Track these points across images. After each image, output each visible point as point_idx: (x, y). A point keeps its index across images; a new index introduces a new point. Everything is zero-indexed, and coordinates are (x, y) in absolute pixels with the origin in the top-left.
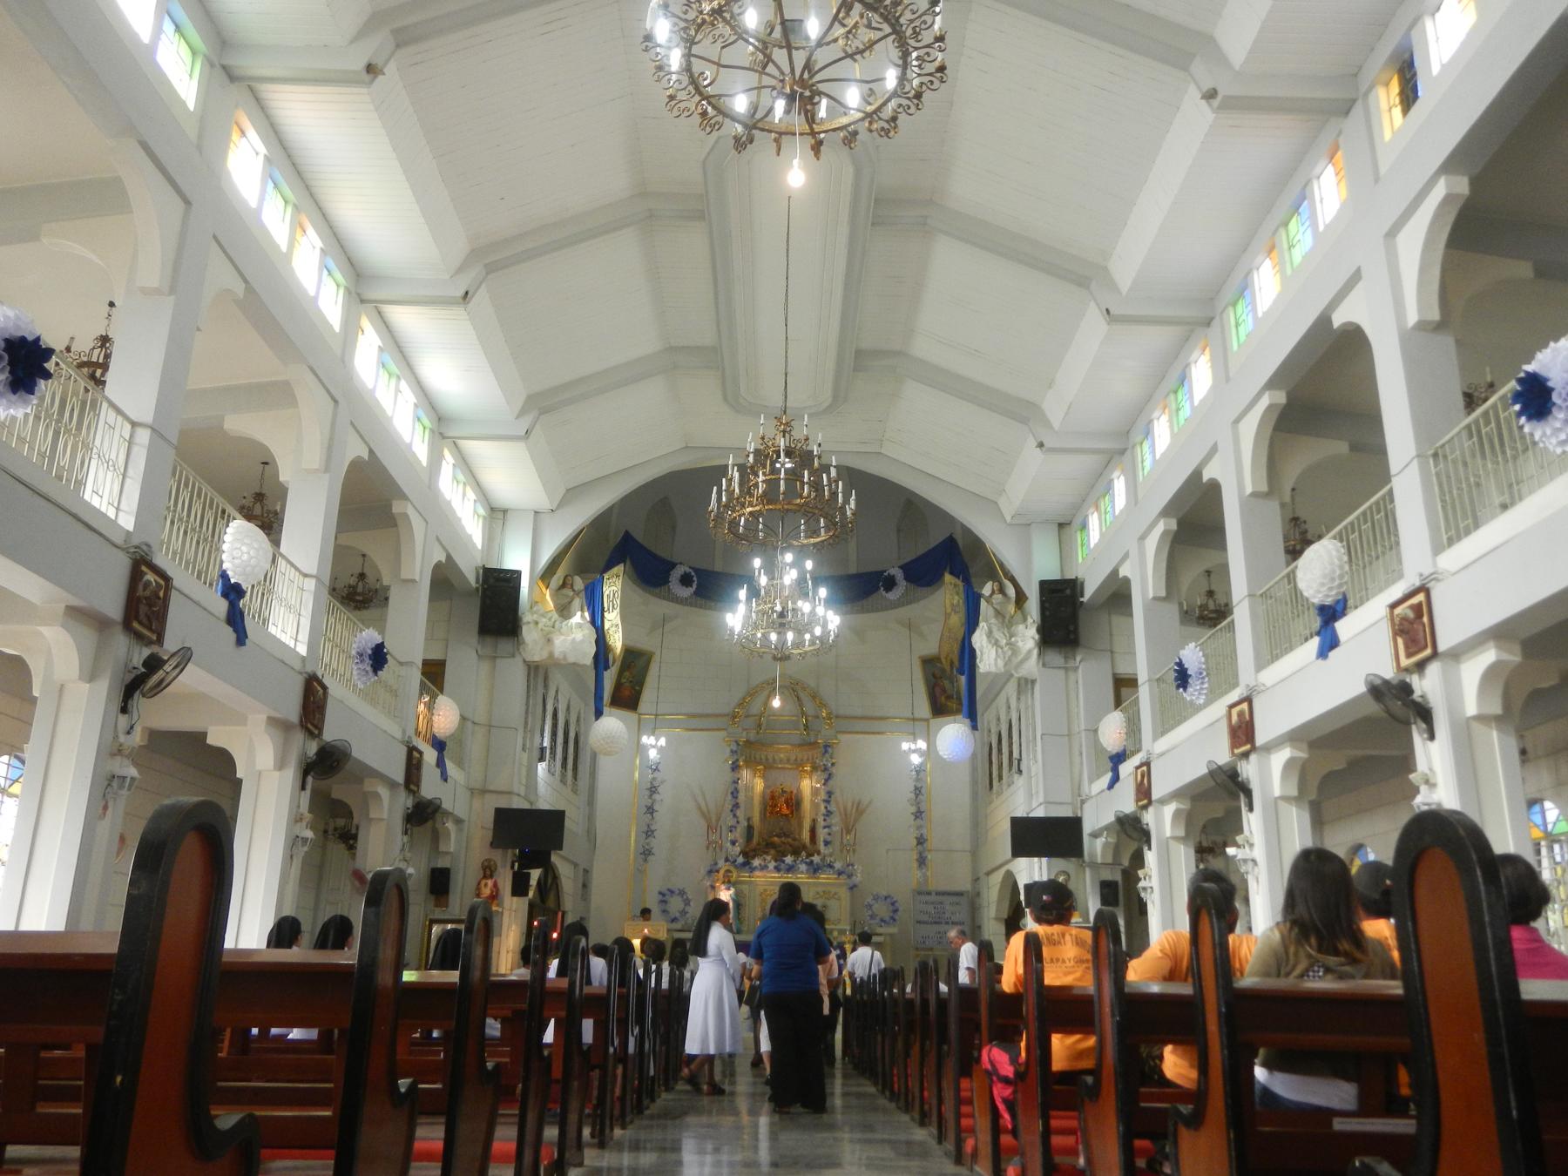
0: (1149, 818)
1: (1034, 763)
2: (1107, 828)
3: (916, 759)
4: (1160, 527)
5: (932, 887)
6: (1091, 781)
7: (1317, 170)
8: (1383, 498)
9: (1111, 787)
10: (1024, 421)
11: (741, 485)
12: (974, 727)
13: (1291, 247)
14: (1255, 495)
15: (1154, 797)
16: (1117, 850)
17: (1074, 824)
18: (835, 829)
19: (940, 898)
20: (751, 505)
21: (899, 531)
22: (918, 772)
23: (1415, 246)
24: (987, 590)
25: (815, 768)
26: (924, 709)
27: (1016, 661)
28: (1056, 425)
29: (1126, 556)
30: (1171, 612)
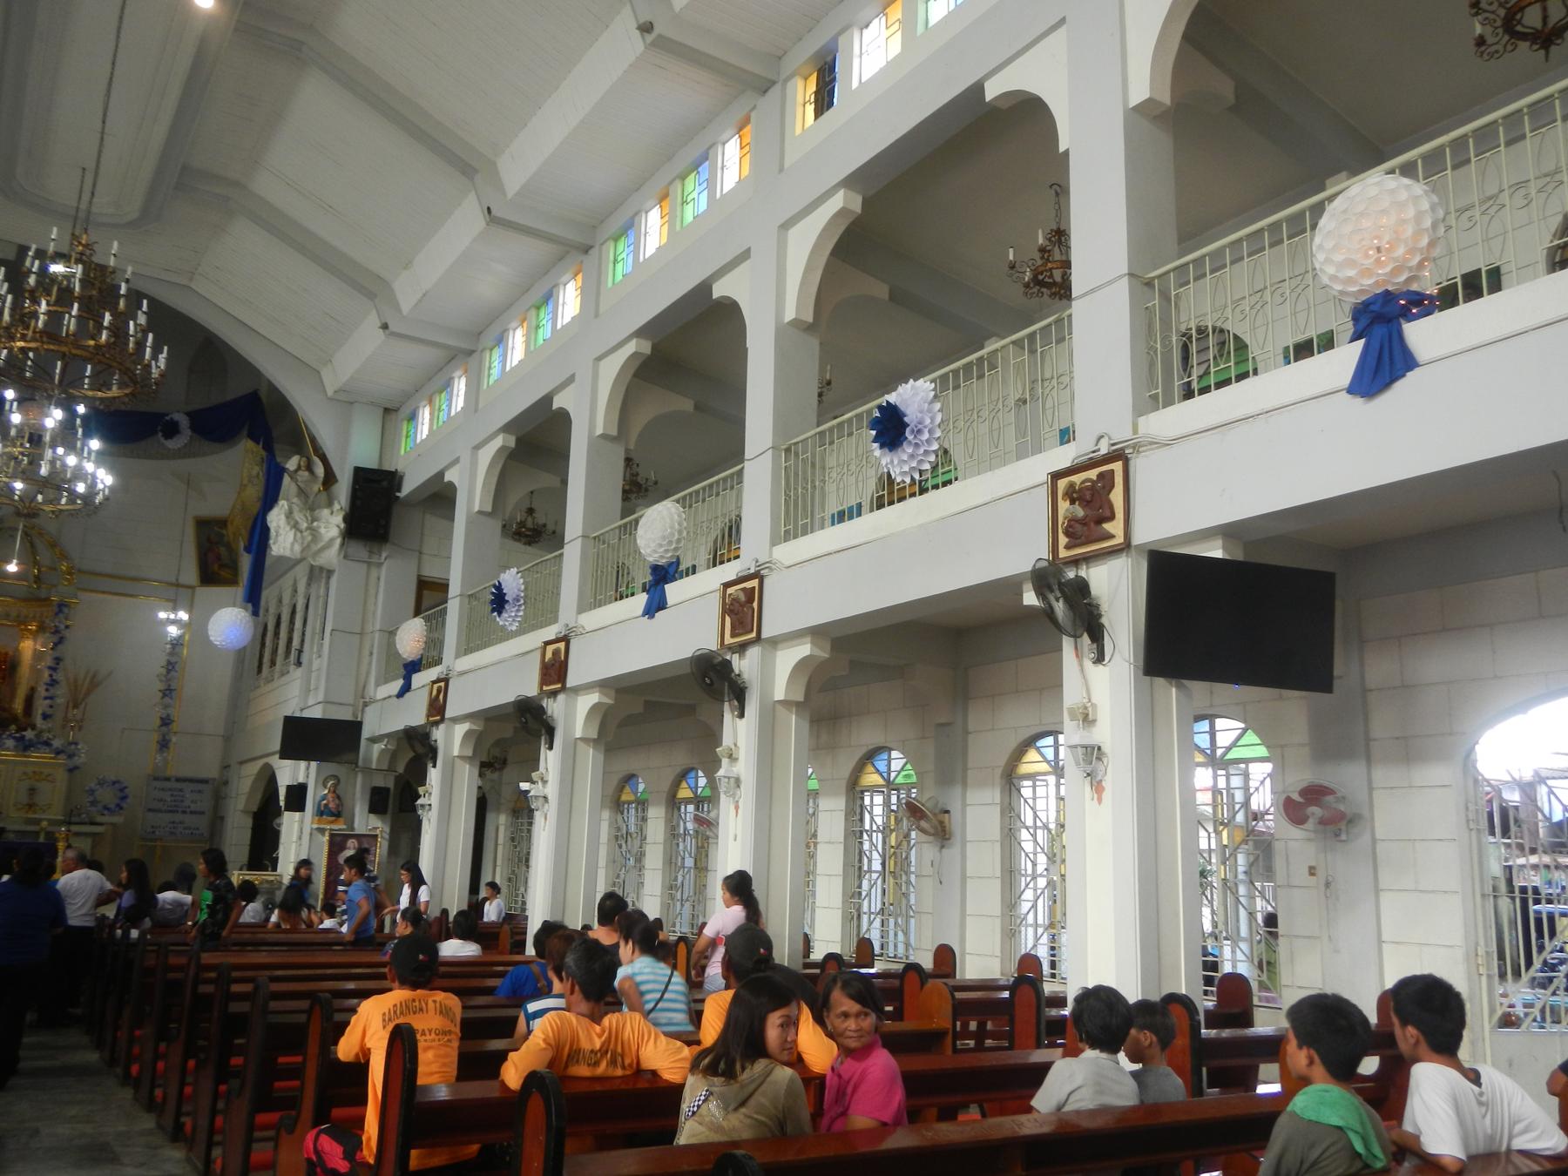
0: (438, 734)
1: (319, 658)
2: (388, 735)
3: (173, 631)
4: (498, 442)
5: (170, 772)
6: (378, 685)
7: (724, 137)
8: (732, 475)
9: (400, 695)
10: (371, 296)
11: (13, 309)
12: (255, 613)
13: (684, 202)
14: (603, 436)
15: (447, 715)
16: (394, 756)
17: (355, 727)
18: (59, 701)
19: (178, 785)
20: (23, 338)
23: (804, 246)
24: (292, 464)
25: (42, 628)
26: (191, 574)
27: (315, 548)
28: (406, 305)
29: (456, 461)
30: (496, 525)
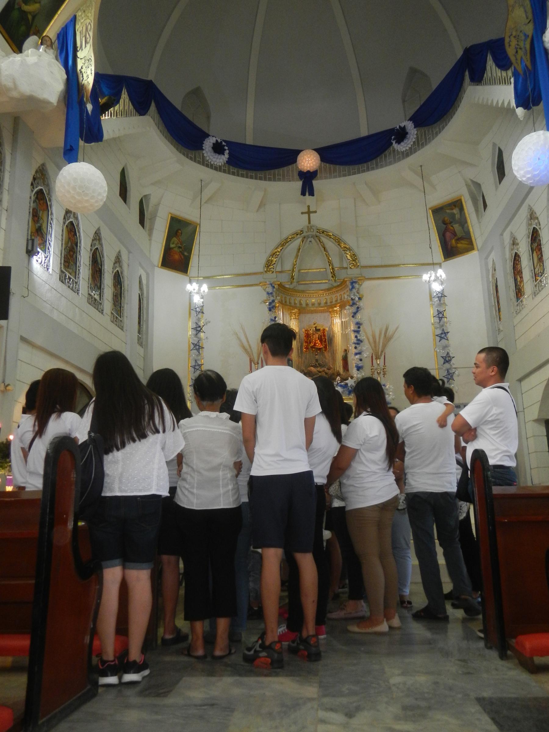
3: (437, 287)
21: (404, 101)
22: (440, 298)
25: (342, 307)
